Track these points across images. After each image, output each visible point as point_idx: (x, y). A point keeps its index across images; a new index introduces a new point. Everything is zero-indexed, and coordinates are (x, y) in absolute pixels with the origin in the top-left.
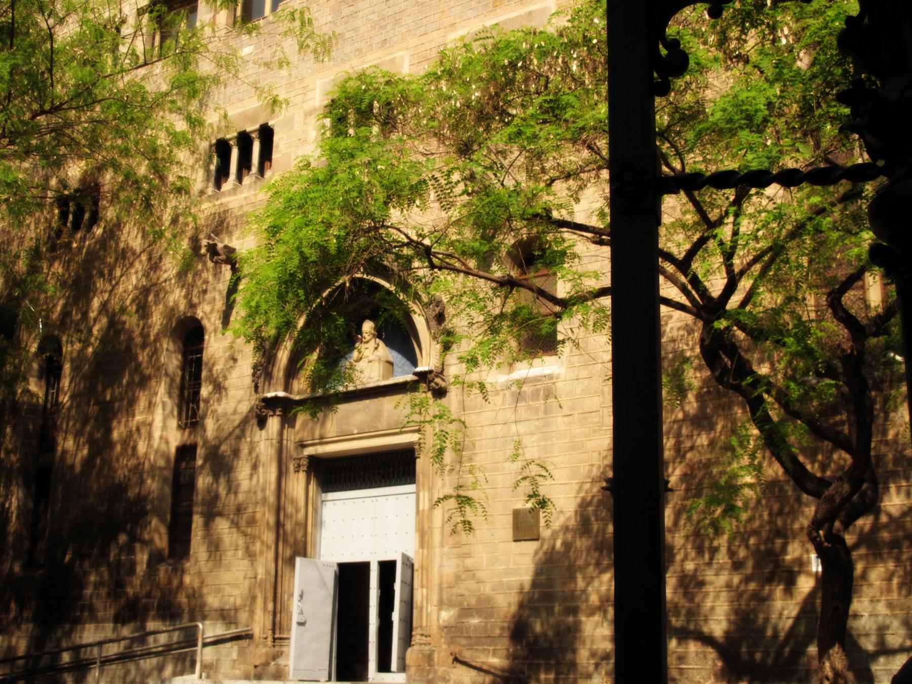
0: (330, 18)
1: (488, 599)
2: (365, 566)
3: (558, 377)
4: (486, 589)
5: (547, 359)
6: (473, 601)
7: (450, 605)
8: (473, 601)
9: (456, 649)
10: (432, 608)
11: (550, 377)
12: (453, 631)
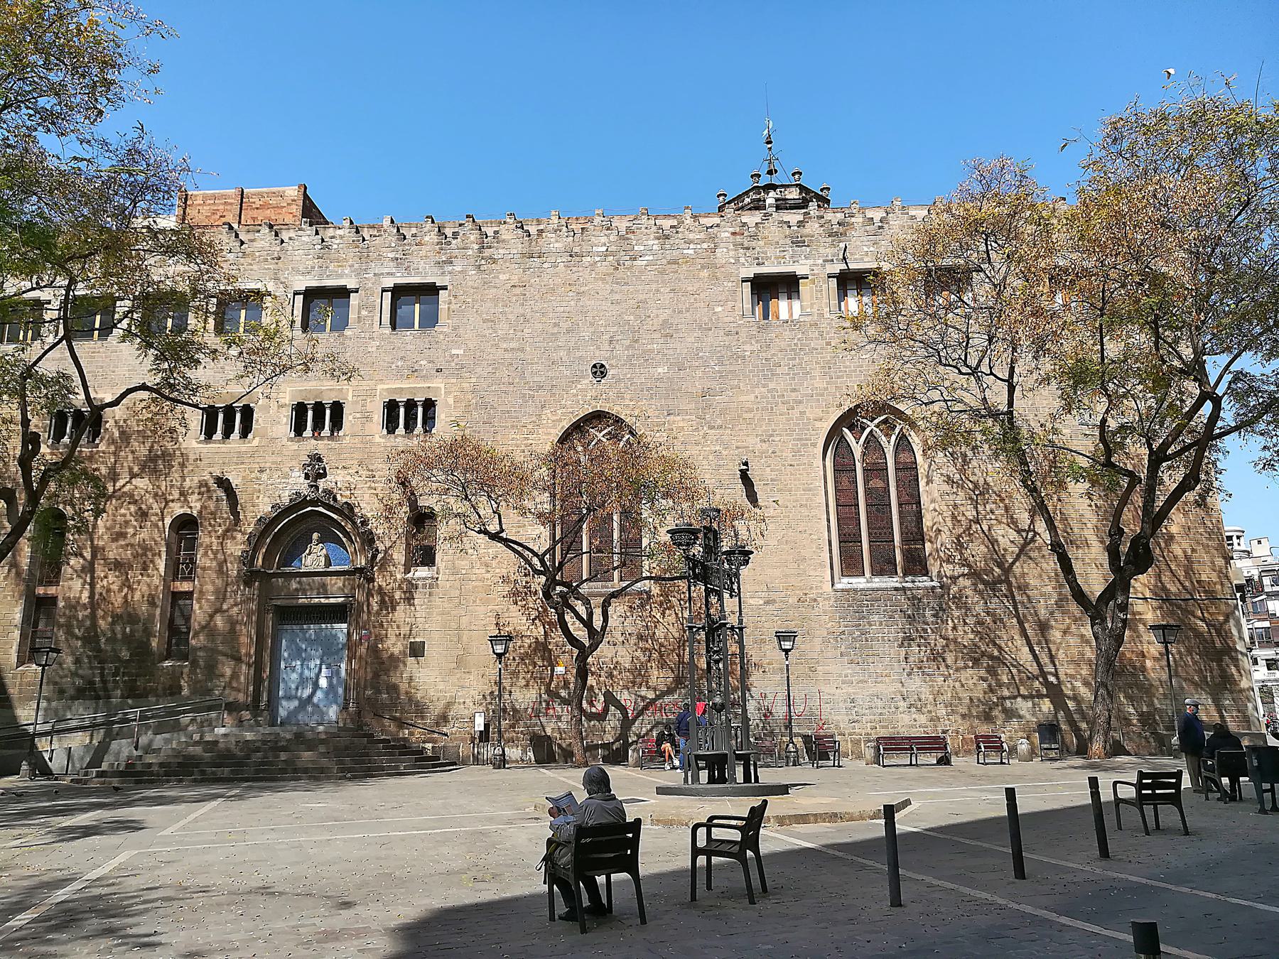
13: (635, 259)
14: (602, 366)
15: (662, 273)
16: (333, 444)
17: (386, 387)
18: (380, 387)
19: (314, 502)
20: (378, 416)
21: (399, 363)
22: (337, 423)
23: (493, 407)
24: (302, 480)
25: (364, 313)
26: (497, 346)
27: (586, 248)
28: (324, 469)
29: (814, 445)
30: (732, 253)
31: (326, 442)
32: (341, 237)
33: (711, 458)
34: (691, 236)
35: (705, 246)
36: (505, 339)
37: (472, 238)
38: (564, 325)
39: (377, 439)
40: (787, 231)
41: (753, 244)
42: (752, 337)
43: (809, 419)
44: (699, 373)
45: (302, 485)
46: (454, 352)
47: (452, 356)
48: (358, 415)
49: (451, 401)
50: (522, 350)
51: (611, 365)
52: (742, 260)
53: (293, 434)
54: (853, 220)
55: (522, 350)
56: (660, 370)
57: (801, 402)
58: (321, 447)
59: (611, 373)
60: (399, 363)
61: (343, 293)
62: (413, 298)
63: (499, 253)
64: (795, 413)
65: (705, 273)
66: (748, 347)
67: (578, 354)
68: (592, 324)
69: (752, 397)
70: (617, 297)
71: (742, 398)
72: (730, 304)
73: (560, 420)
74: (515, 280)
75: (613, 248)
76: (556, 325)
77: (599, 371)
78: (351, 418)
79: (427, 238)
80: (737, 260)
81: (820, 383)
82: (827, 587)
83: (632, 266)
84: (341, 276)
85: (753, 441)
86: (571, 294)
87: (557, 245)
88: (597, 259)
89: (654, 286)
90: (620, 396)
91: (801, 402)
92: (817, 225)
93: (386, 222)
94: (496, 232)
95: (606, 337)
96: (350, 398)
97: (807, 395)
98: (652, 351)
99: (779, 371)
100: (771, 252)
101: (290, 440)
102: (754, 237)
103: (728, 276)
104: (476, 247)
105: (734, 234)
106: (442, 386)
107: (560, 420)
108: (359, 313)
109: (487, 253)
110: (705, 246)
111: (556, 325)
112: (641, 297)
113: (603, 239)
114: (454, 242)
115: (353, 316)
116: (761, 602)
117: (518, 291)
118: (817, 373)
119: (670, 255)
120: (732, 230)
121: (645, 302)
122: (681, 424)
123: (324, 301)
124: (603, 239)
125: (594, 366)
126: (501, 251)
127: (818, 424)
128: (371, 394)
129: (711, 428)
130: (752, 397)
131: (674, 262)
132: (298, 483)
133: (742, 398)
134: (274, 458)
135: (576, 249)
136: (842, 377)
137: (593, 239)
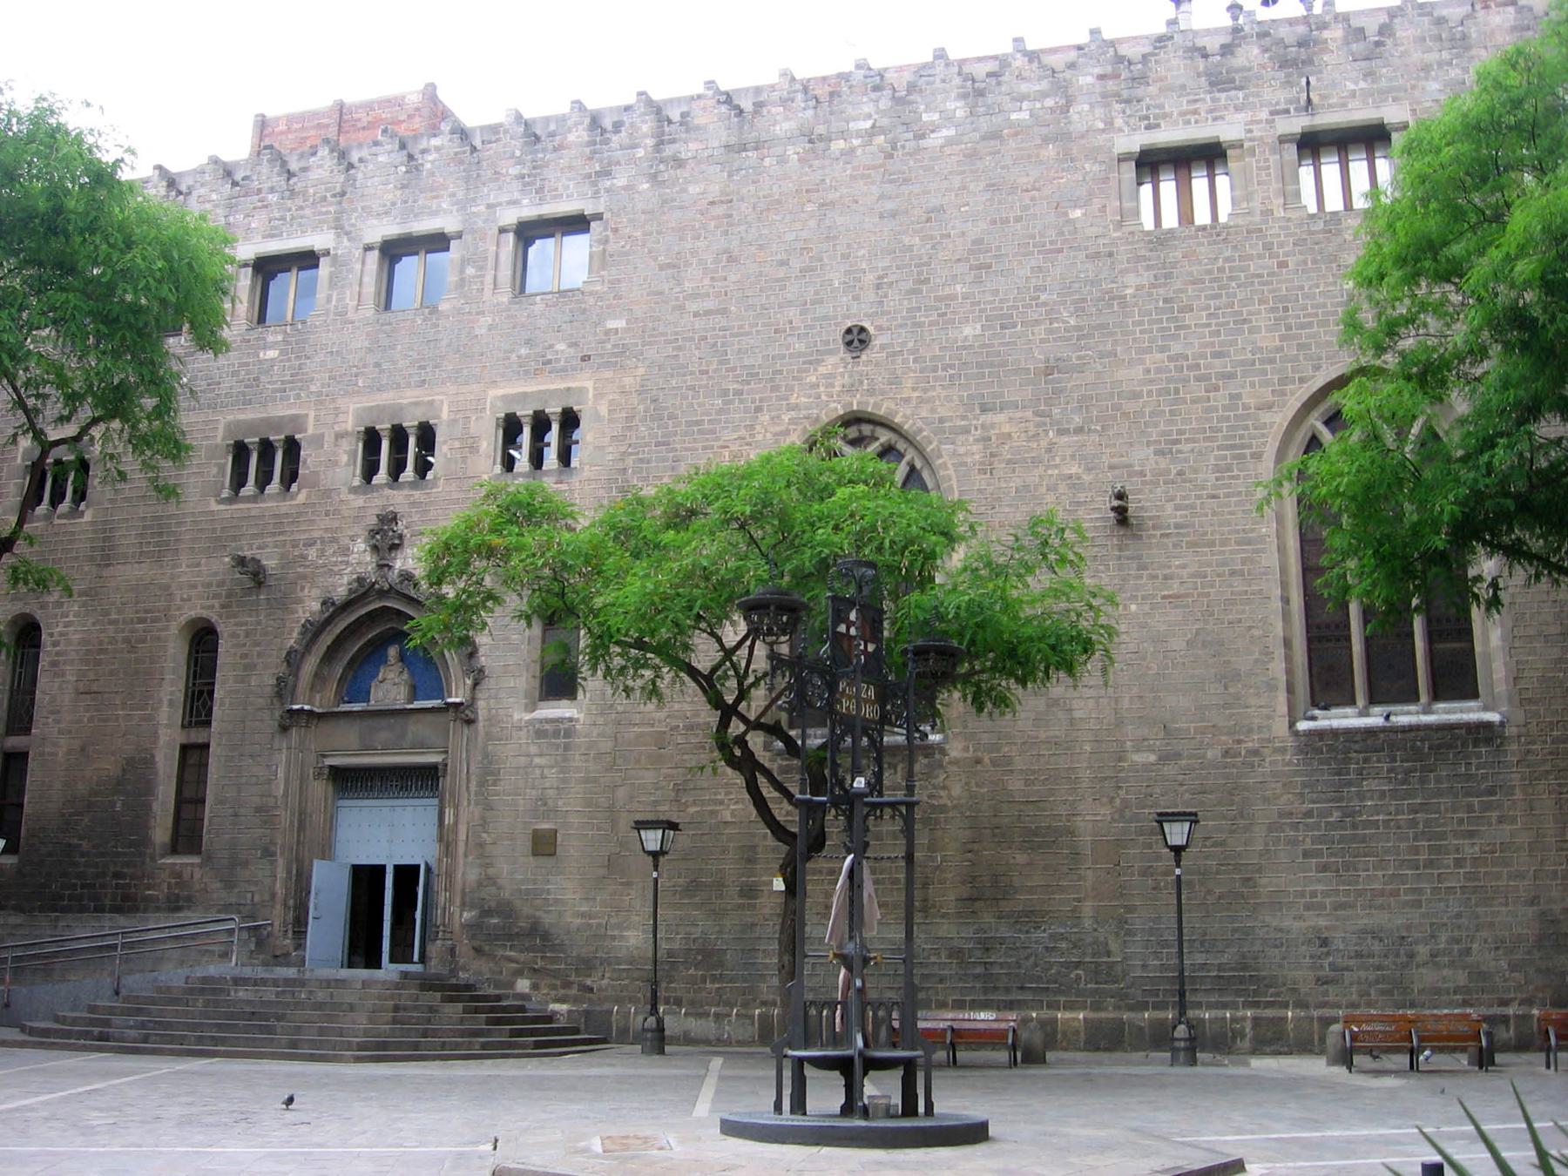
0: (366, 344)
1: (509, 903)
2: (380, 870)
3: (577, 720)
4: (506, 895)
5: (565, 702)
6: (493, 904)
7: (472, 907)
8: (493, 904)
9: (477, 943)
10: (455, 909)
11: (571, 720)
12: (473, 928)
13: (923, 137)
14: (862, 330)
15: (973, 155)
16: (417, 494)
17: (501, 392)
18: (494, 393)
19: (382, 594)
21: (523, 351)
23: (672, 416)
25: (470, 271)
26: (681, 307)
27: (836, 125)
28: (401, 537)
29: (1257, 456)
30: (1099, 112)
32: (438, 149)
33: (1062, 488)
34: (1024, 88)
35: (1049, 102)
36: (695, 296)
37: (645, 128)
38: (796, 264)
40: (1201, 64)
41: (1140, 92)
42: (1139, 259)
43: (1246, 407)
44: (1040, 332)
46: (612, 324)
47: (608, 332)
48: (457, 444)
49: (603, 410)
50: (724, 312)
51: (879, 328)
52: (1119, 122)
53: (357, 481)
54: (1326, 34)
55: (724, 312)
56: (968, 331)
57: (1231, 376)
58: (397, 499)
59: (876, 343)
60: (523, 351)
64: (1220, 399)
65: (1051, 150)
66: (1131, 280)
67: (820, 311)
68: (845, 257)
69: (1137, 372)
70: (890, 205)
71: (1122, 374)
72: (1097, 203)
73: (787, 433)
74: (715, 190)
75: (885, 122)
77: (856, 339)
78: (445, 448)
79: (571, 137)
80: (1109, 123)
81: (1268, 340)
82: (1280, 727)
83: (918, 150)
84: (435, 214)
85: (1142, 456)
86: (809, 208)
87: (786, 126)
88: (856, 142)
89: (956, 181)
90: (895, 381)
91: (1231, 376)
92: (1256, 51)
94: (684, 115)
95: (870, 278)
96: (445, 415)
97: (1242, 363)
98: (953, 297)
99: (1189, 319)
100: (1172, 105)
101: (354, 490)
102: (1141, 79)
103: (1092, 154)
104: (650, 142)
105: (1101, 77)
106: (589, 384)
107: (787, 433)
109: (668, 151)
110: (1049, 102)
112: (934, 202)
113: (868, 108)
114: (615, 138)
116: (1153, 758)
117: (719, 210)
118: (1262, 320)
119: (984, 124)
120: (1097, 71)
121: (940, 209)
122: (1006, 429)
124: (868, 108)
125: (849, 331)
127: (1266, 417)
129: (1061, 432)
130: (1137, 372)
131: (995, 135)
132: (361, 558)
133: (1122, 374)
134: (326, 522)
135: (821, 129)
136: (1310, 325)
137: (850, 110)
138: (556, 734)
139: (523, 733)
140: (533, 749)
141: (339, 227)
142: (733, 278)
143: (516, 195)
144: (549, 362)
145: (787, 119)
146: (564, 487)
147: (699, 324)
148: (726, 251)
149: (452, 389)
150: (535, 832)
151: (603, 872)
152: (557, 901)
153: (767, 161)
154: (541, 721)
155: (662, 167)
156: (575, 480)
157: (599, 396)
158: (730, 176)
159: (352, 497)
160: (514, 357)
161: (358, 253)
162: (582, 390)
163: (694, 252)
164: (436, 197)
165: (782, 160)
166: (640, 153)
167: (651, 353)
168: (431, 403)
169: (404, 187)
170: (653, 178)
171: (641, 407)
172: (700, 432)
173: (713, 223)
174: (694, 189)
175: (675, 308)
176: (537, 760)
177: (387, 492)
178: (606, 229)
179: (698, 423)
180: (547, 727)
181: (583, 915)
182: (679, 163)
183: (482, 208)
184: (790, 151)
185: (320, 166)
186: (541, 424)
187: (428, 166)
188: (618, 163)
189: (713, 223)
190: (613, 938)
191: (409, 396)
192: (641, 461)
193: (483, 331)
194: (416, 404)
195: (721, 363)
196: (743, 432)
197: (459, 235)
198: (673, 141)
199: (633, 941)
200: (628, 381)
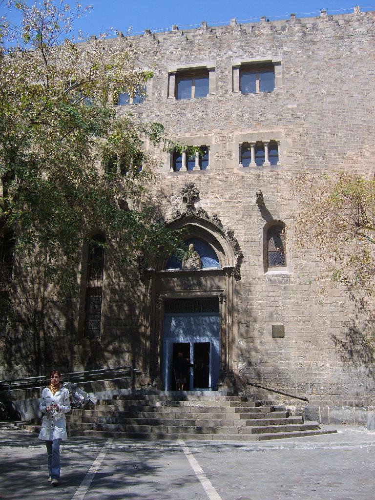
3: (290, 275)
5: (280, 268)
11: (287, 275)
16: (202, 176)
17: (240, 133)
18: (235, 134)
20: (235, 155)
21: (249, 116)
22: (203, 162)
24: (181, 203)
31: (197, 175)
36: (328, 96)
39: (236, 171)
45: (183, 208)
46: (290, 106)
49: (290, 141)
50: (342, 102)
53: (172, 170)
58: (194, 177)
60: (249, 116)
61: (203, 73)
62: (256, 72)
63: (317, 38)
74: (332, 55)
76: (366, 83)
79: (263, 31)
84: (203, 59)
87: (361, 30)
93: (233, 24)
94: (314, 25)
96: (213, 142)
101: (170, 174)
104: (300, 34)
106: (282, 131)
108: (217, 83)
109: (309, 38)
111: (366, 83)
114: (283, 33)
115: (212, 86)
117: (335, 62)
123: (191, 78)
126: (319, 36)
128: (230, 138)
138: (280, 282)
139: (264, 282)
140: (270, 289)
141: (156, 65)
142: (344, 89)
143: (239, 54)
144: (262, 121)
145: (360, 27)
146: (273, 173)
147: (330, 107)
148: (340, 78)
149: (217, 131)
150: (273, 327)
151: (308, 344)
152: (286, 359)
153: (354, 43)
154: (272, 276)
155: (306, 44)
156: (279, 170)
157: (287, 135)
158: (338, 48)
159: (170, 177)
160: (245, 119)
161: (166, 76)
162: (279, 133)
163: (325, 78)
164: (202, 54)
165: (361, 43)
166: (296, 38)
167: (309, 118)
168: (206, 137)
169: (185, 49)
170: (302, 48)
171: (308, 140)
172: (336, 151)
173: (332, 67)
174: (321, 53)
175: (319, 101)
176: (271, 294)
177: (188, 175)
178: (283, 68)
179: (335, 147)
180: (276, 278)
181: (300, 364)
182: (313, 43)
183: (224, 58)
184: (364, 39)
185: (145, 41)
186: (259, 146)
187: (197, 41)
188: (286, 42)
189: (332, 67)
190: (316, 375)
191: (195, 134)
192: (311, 163)
193: (229, 108)
194: (199, 138)
195: (343, 123)
196: (357, 151)
197: (213, 69)
198: (311, 34)
199: (326, 376)
200: (300, 129)
